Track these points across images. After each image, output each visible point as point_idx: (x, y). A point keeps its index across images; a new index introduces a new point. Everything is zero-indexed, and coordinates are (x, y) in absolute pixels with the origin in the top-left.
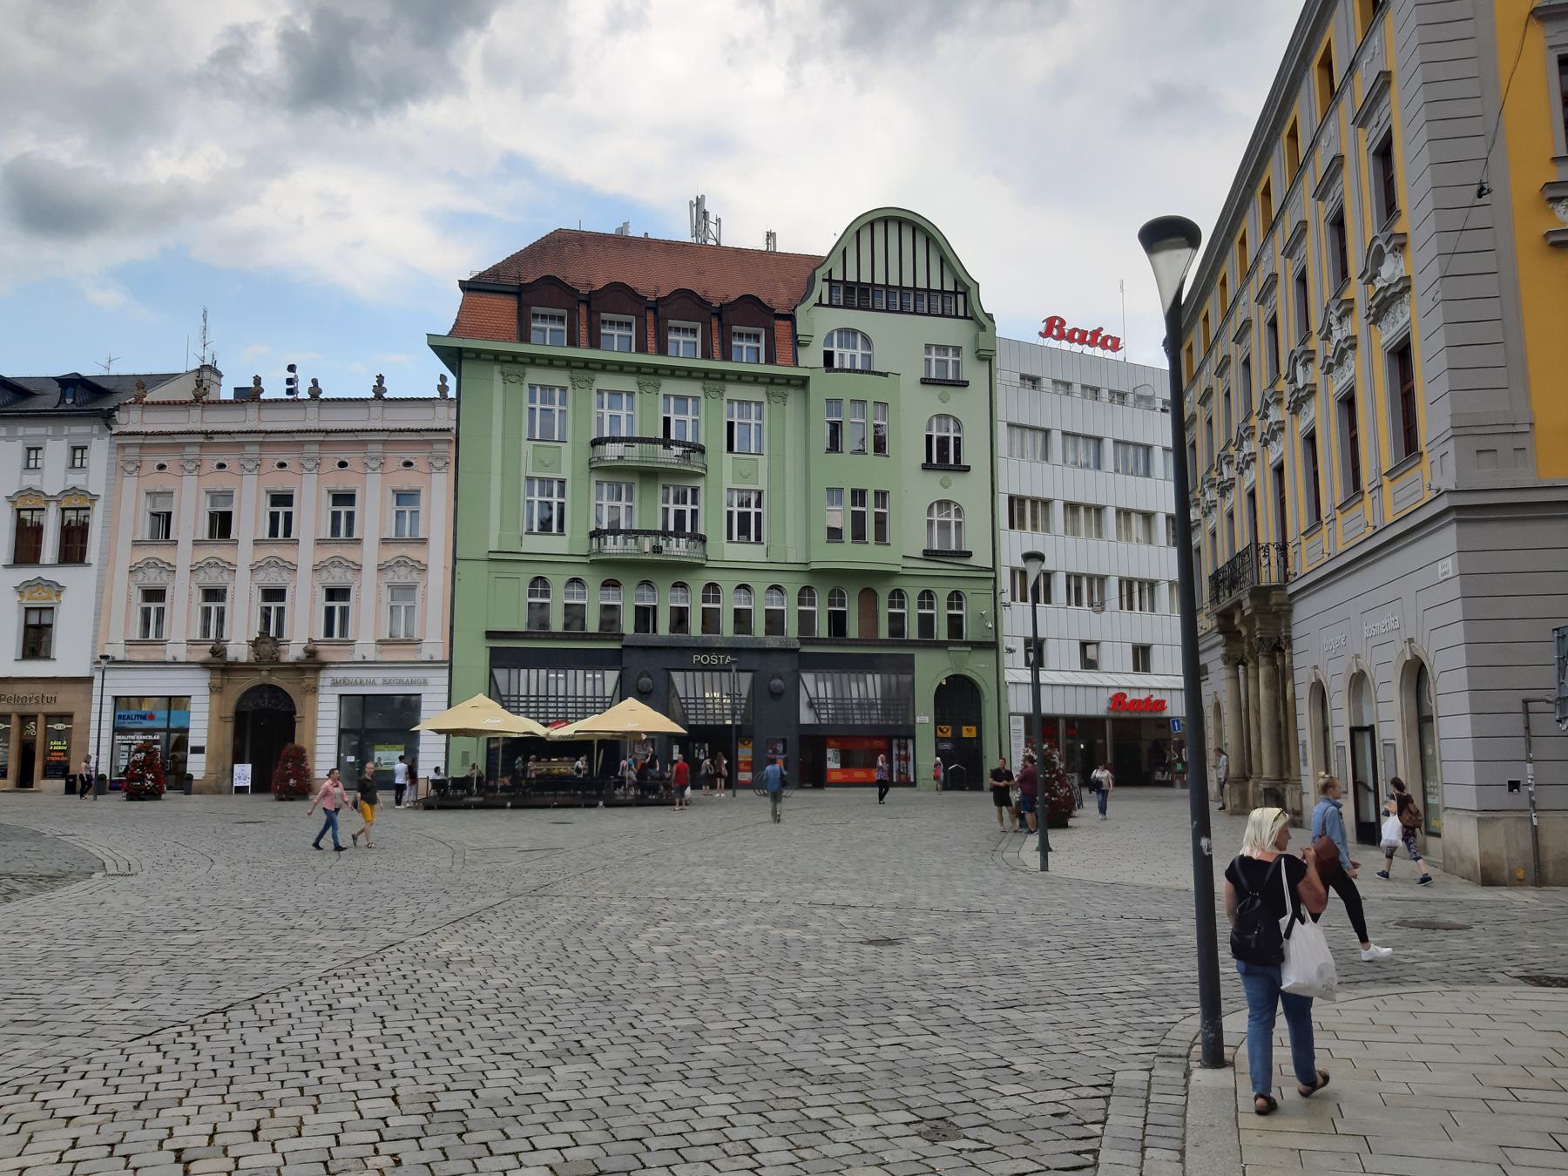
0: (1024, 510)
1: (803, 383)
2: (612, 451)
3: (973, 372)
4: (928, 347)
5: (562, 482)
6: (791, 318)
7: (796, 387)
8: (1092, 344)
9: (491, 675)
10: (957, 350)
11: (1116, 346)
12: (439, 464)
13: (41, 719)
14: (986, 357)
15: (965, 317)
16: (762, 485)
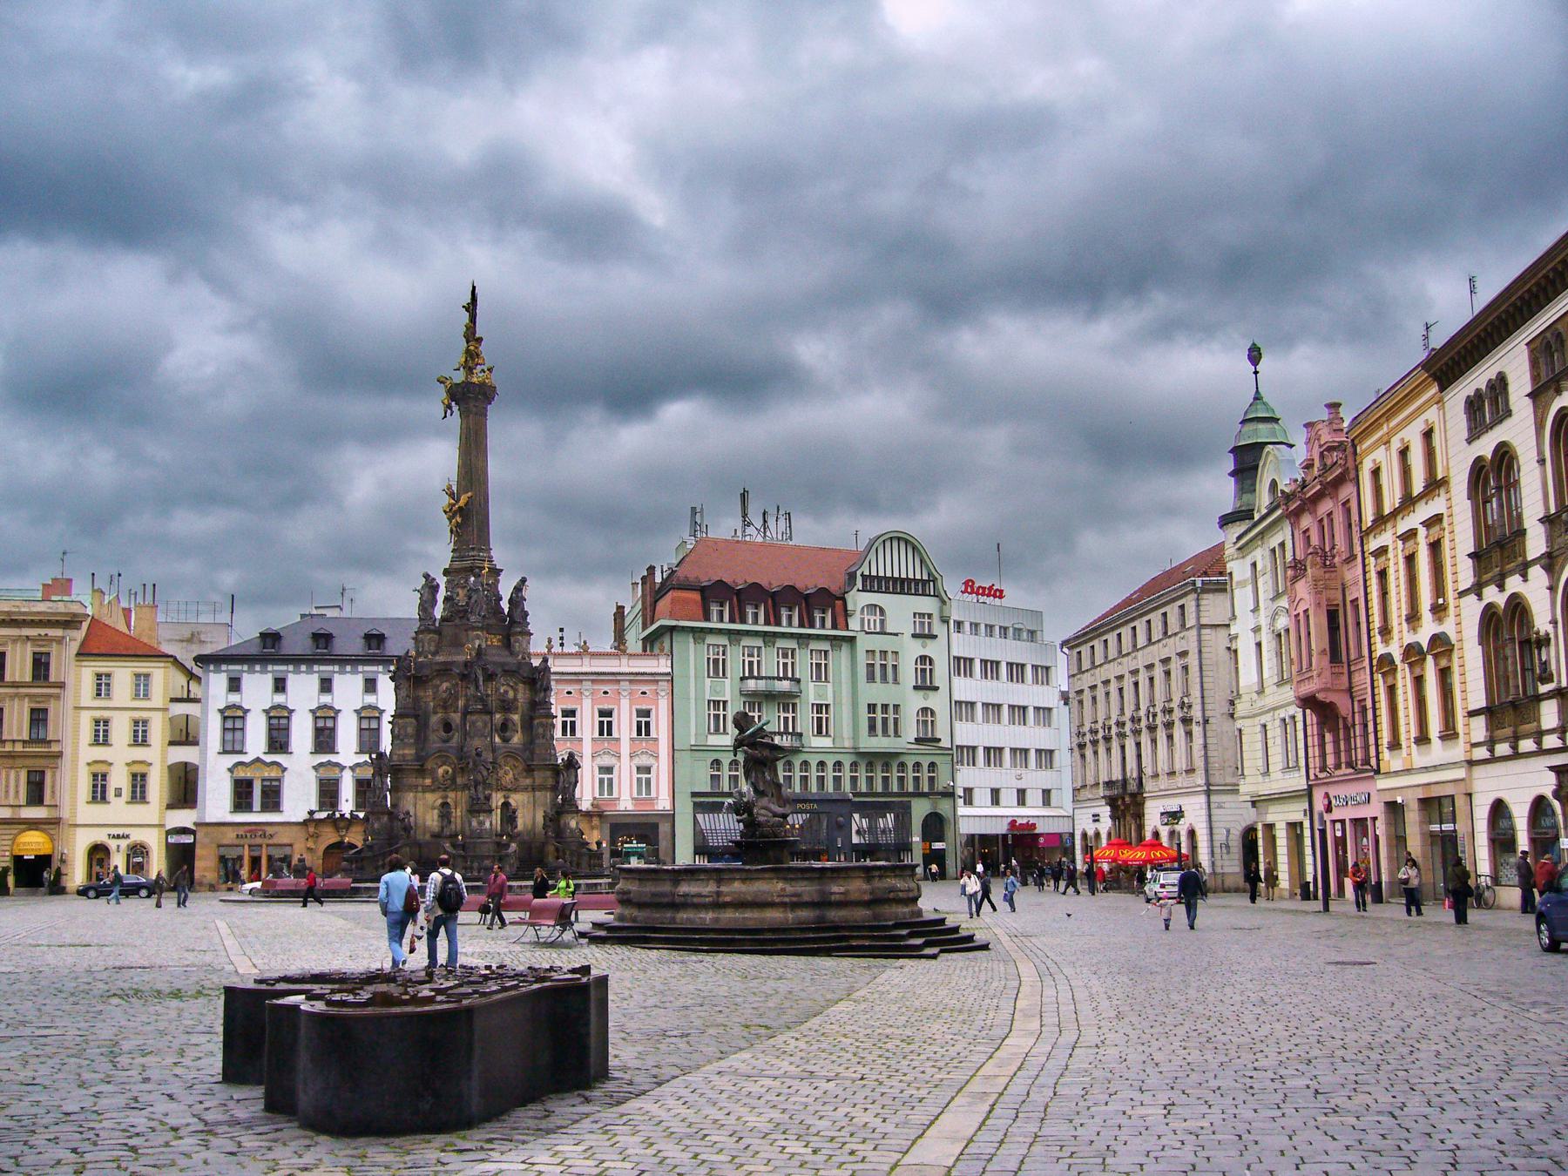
0: (964, 708)
1: (852, 640)
2: (751, 685)
3: (939, 628)
4: (915, 614)
5: (725, 702)
6: (844, 600)
7: (846, 641)
8: (988, 595)
9: (695, 816)
10: (930, 616)
11: (1001, 597)
12: (663, 694)
13: (264, 846)
14: (945, 620)
15: (934, 596)
16: (830, 701)
